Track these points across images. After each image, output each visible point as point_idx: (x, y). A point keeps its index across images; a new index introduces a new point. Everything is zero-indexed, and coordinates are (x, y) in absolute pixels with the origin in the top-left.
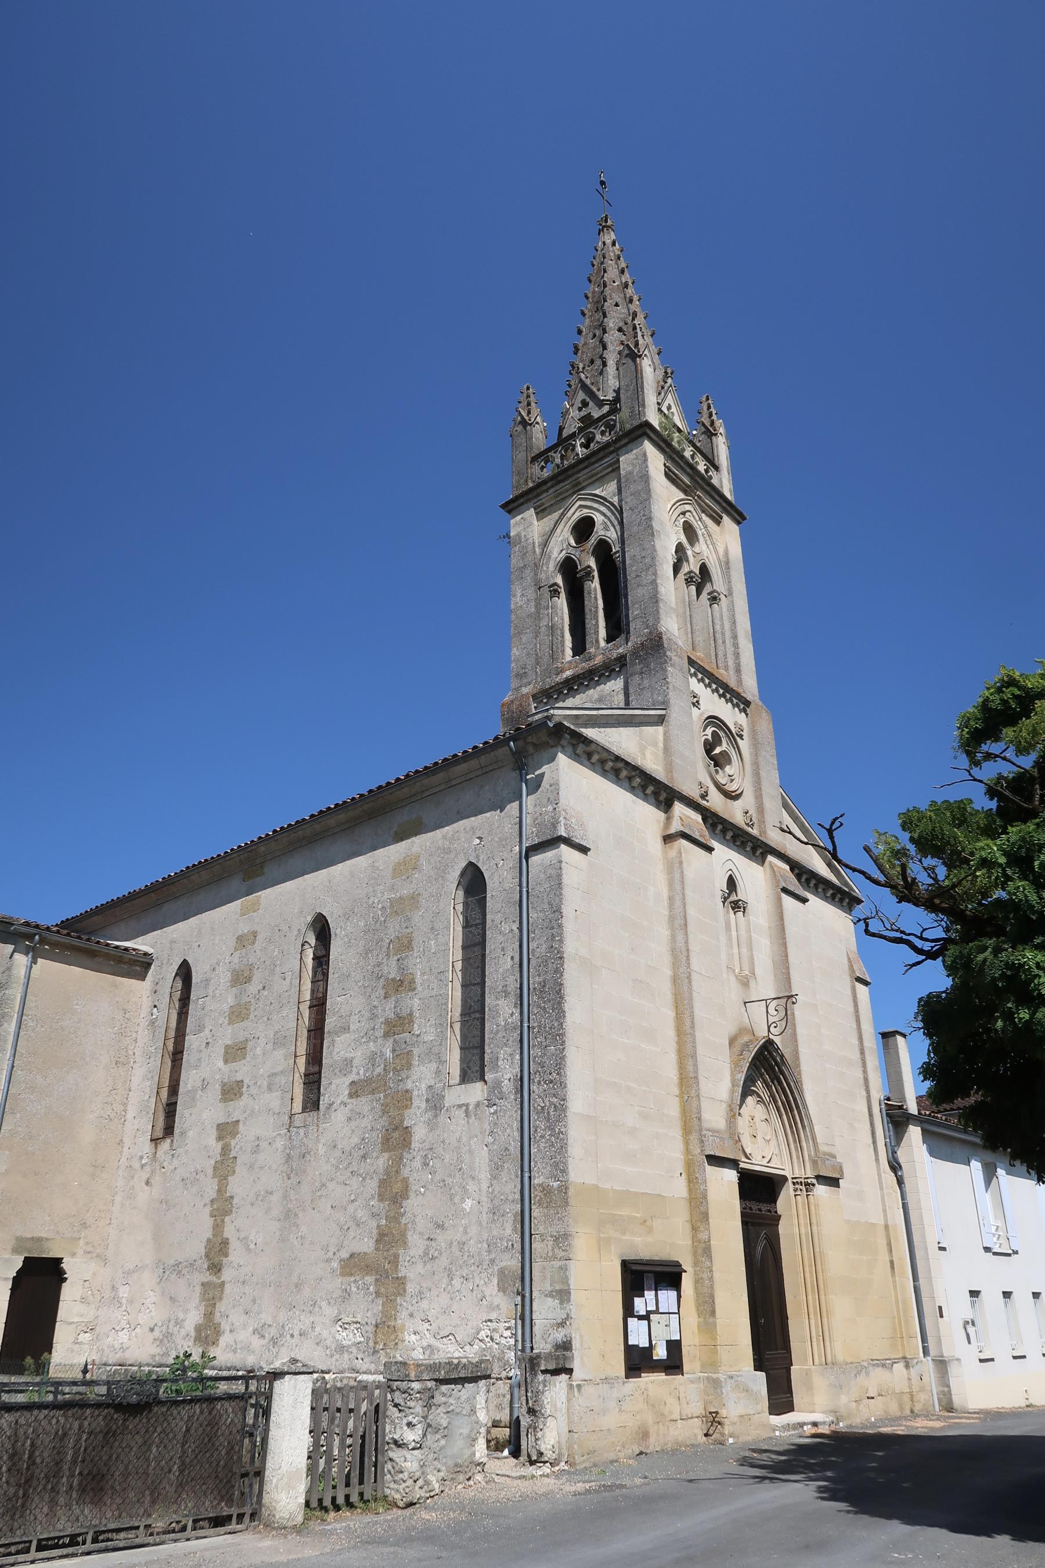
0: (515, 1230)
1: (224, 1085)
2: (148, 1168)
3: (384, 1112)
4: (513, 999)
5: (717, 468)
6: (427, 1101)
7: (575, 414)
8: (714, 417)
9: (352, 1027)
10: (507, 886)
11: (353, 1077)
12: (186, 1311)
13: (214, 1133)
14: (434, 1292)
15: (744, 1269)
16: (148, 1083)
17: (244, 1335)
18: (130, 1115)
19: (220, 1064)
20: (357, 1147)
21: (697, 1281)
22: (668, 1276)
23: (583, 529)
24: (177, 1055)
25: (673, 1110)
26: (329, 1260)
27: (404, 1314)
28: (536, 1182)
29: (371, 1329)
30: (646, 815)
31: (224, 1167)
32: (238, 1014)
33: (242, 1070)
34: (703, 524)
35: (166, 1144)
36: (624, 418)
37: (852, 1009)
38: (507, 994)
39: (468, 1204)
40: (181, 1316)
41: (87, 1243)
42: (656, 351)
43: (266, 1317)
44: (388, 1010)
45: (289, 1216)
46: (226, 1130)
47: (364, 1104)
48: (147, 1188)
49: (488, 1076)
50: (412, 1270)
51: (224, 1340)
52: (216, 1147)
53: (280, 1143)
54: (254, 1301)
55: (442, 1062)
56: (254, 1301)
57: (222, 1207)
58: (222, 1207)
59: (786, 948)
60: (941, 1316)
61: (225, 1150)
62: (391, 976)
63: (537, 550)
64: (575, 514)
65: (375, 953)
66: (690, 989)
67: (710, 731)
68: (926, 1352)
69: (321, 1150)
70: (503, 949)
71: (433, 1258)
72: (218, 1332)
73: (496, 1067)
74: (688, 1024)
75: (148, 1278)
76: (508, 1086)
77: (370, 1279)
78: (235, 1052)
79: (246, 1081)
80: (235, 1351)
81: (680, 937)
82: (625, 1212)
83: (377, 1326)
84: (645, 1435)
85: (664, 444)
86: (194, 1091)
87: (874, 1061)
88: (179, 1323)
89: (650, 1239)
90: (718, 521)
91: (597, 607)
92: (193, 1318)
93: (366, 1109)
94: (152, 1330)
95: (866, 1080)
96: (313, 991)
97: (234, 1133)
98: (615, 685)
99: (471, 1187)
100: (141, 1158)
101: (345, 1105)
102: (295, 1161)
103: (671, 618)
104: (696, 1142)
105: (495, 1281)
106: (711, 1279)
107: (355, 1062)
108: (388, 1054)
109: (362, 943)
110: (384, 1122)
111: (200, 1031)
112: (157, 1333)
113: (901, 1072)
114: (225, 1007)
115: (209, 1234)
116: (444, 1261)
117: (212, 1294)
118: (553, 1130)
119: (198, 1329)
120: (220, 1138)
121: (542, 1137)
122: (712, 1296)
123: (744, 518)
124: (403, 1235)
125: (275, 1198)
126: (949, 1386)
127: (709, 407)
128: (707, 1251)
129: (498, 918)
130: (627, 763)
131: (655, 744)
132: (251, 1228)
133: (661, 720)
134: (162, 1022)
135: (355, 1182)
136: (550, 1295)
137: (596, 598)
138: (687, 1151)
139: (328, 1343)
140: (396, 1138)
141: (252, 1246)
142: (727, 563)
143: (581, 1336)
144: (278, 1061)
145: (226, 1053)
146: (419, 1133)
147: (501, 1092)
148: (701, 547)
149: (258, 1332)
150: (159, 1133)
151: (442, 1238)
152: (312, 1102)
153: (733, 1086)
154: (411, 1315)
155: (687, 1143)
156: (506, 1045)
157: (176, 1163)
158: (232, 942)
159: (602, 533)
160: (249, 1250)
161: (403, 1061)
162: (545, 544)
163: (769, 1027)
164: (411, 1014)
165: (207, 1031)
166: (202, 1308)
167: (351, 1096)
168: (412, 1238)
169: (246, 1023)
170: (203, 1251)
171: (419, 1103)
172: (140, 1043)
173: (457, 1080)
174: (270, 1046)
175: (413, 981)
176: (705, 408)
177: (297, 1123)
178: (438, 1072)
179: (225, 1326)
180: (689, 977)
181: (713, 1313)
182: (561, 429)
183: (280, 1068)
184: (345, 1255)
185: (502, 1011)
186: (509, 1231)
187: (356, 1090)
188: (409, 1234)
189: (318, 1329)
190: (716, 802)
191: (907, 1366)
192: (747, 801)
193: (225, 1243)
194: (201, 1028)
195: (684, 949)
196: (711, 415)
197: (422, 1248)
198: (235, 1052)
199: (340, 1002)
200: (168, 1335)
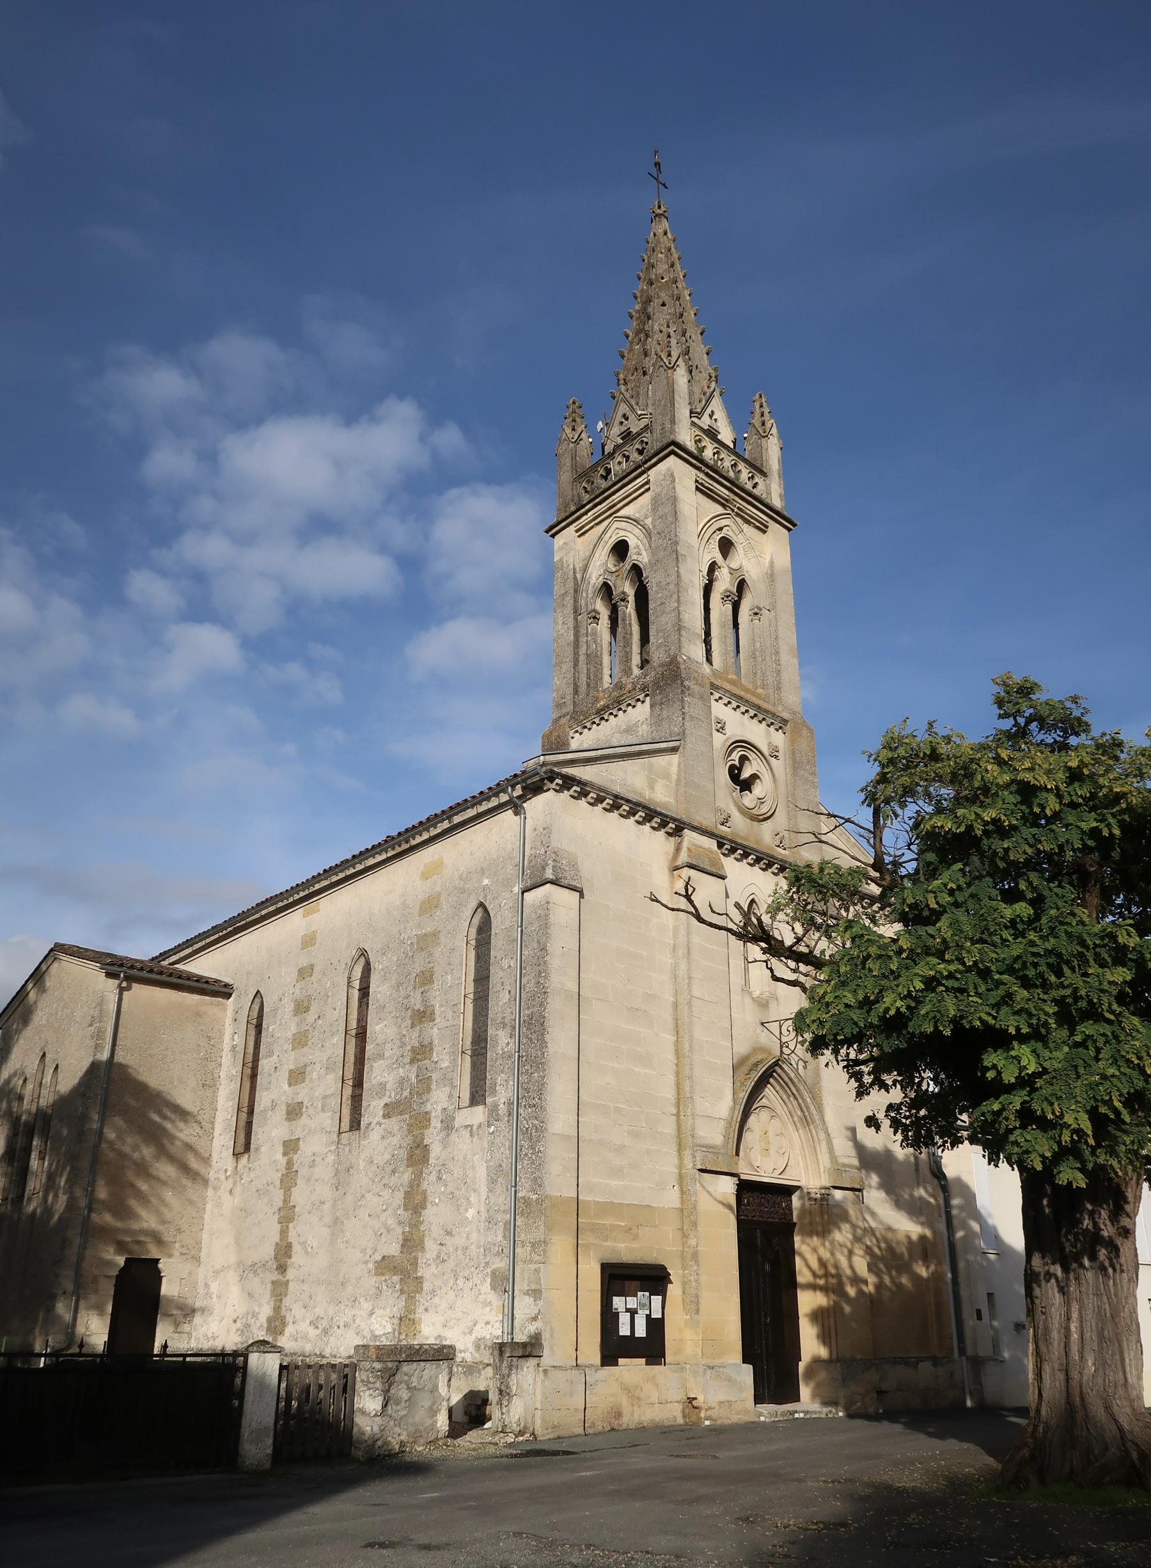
0: (504, 1237)
1: (288, 1105)
2: (230, 1180)
3: (410, 1131)
4: (508, 1029)
5: (764, 474)
6: (442, 1121)
7: (616, 430)
8: (767, 416)
9: (387, 1054)
10: (507, 924)
11: (386, 1100)
12: (260, 1306)
13: (281, 1149)
14: (444, 1290)
16: (231, 1104)
17: (304, 1326)
18: (216, 1133)
19: (286, 1087)
20: (388, 1163)
21: (685, 1284)
22: (654, 1279)
23: (621, 549)
24: (254, 1076)
25: (668, 1127)
26: (366, 1262)
27: (421, 1309)
28: (520, 1195)
29: (396, 1321)
30: (654, 845)
31: (289, 1178)
32: (300, 1041)
33: (302, 1093)
34: (743, 536)
35: (244, 1160)
36: (654, 441)
38: (504, 1025)
39: (470, 1213)
40: (257, 1309)
41: (183, 1246)
42: (705, 351)
43: (319, 1311)
44: (413, 1039)
45: (336, 1223)
46: (291, 1147)
47: (394, 1124)
48: (231, 1198)
49: (489, 1100)
50: (428, 1272)
51: (289, 1330)
52: (283, 1161)
53: (331, 1158)
54: (311, 1297)
55: (453, 1087)
56: (311, 1297)
57: (287, 1214)
58: (287, 1214)
61: (290, 1164)
62: (417, 1008)
63: (579, 576)
64: (611, 539)
65: (405, 986)
67: (736, 756)
68: (962, 1351)
69: (362, 1164)
70: (502, 984)
71: (443, 1261)
72: (284, 1324)
73: (494, 1092)
74: (687, 1047)
75: (232, 1276)
76: (502, 1109)
77: (396, 1278)
78: (297, 1076)
79: (305, 1103)
80: (296, 1340)
81: (683, 966)
82: (608, 1221)
83: (401, 1319)
84: (619, 1415)
85: (695, 460)
86: (265, 1111)
88: (255, 1315)
89: (634, 1245)
90: (763, 529)
91: (631, 634)
92: (266, 1311)
93: (396, 1128)
94: (235, 1321)
96: (358, 1020)
97: (296, 1149)
98: (641, 712)
99: (473, 1198)
100: (226, 1171)
101: (380, 1124)
102: (343, 1173)
103: (695, 644)
104: (690, 1157)
105: (489, 1280)
106: (697, 1281)
107: (389, 1086)
108: (414, 1079)
109: (395, 976)
110: (409, 1140)
111: (269, 1056)
112: (239, 1324)
114: (289, 1035)
115: (277, 1239)
116: (451, 1263)
117: (279, 1290)
118: (534, 1149)
119: (270, 1321)
120: (285, 1154)
121: (526, 1155)
122: (697, 1296)
123: (794, 525)
124: (422, 1241)
125: (327, 1206)
127: (761, 406)
128: (695, 1256)
129: (500, 955)
130: (628, 801)
131: (667, 776)
132: (309, 1233)
133: (674, 750)
134: (240, 1049)
135: (386, 1193)
136: (527, 1293)
137: (630, 624)
138: (681, 1166)
139: (365, 1333)
140: (418, 1155)
141: (309, 1249)
142: (772, 575)
143: (552, 1329)
144: (326, 1085)
145: (290, 1076)
146: (436, 1151)
147: (498, 1115)
148: (740, 558)
149: (314, 1324)
150: (240, 1149)
151: (449, 1241)
152: (355, 1124)
154: (426, 1310)
155: (680, 1157)
156: (502, 1072)
157: (252, 1175)
158: (295, 975)
159: (635, 557)
160: (307, 1253)
161: (424, 1085)
162: (585, 569)
163: (781, 1047)
164: (431, 1043)
165: (275, 1057)
166: (272, 1303)
167: (384, 1116)
168: (429, 1243)
169: (305, 1049)
170: (273, 1254)
171: (436, 1123)
172: (224, 1068)
173: (467, 1104)
174: (323, 1071)
175: (433, 1013)
176: (757, 407)
177: (344, 1141)
178: (450, 1096)
179: (289, 1319)
180: (690, 1004)
181: (698, 1311)
182: (603, 446)
183: (330, 1092)
184: (379, 1258)
185: (501, 1041)
186: (500, 1238)
187: (389, 1111)
188: (426, 1239)
189: (357, 1321)
190: (739, 826)
192: (780, 821)
193: (289, 1246)
194: (270, 1054)
195: (686, 976)
196: (762, 415)
197: (435, 1253)
198: (297, 1076)
199: (377, 1029)
200: (247, 1326)
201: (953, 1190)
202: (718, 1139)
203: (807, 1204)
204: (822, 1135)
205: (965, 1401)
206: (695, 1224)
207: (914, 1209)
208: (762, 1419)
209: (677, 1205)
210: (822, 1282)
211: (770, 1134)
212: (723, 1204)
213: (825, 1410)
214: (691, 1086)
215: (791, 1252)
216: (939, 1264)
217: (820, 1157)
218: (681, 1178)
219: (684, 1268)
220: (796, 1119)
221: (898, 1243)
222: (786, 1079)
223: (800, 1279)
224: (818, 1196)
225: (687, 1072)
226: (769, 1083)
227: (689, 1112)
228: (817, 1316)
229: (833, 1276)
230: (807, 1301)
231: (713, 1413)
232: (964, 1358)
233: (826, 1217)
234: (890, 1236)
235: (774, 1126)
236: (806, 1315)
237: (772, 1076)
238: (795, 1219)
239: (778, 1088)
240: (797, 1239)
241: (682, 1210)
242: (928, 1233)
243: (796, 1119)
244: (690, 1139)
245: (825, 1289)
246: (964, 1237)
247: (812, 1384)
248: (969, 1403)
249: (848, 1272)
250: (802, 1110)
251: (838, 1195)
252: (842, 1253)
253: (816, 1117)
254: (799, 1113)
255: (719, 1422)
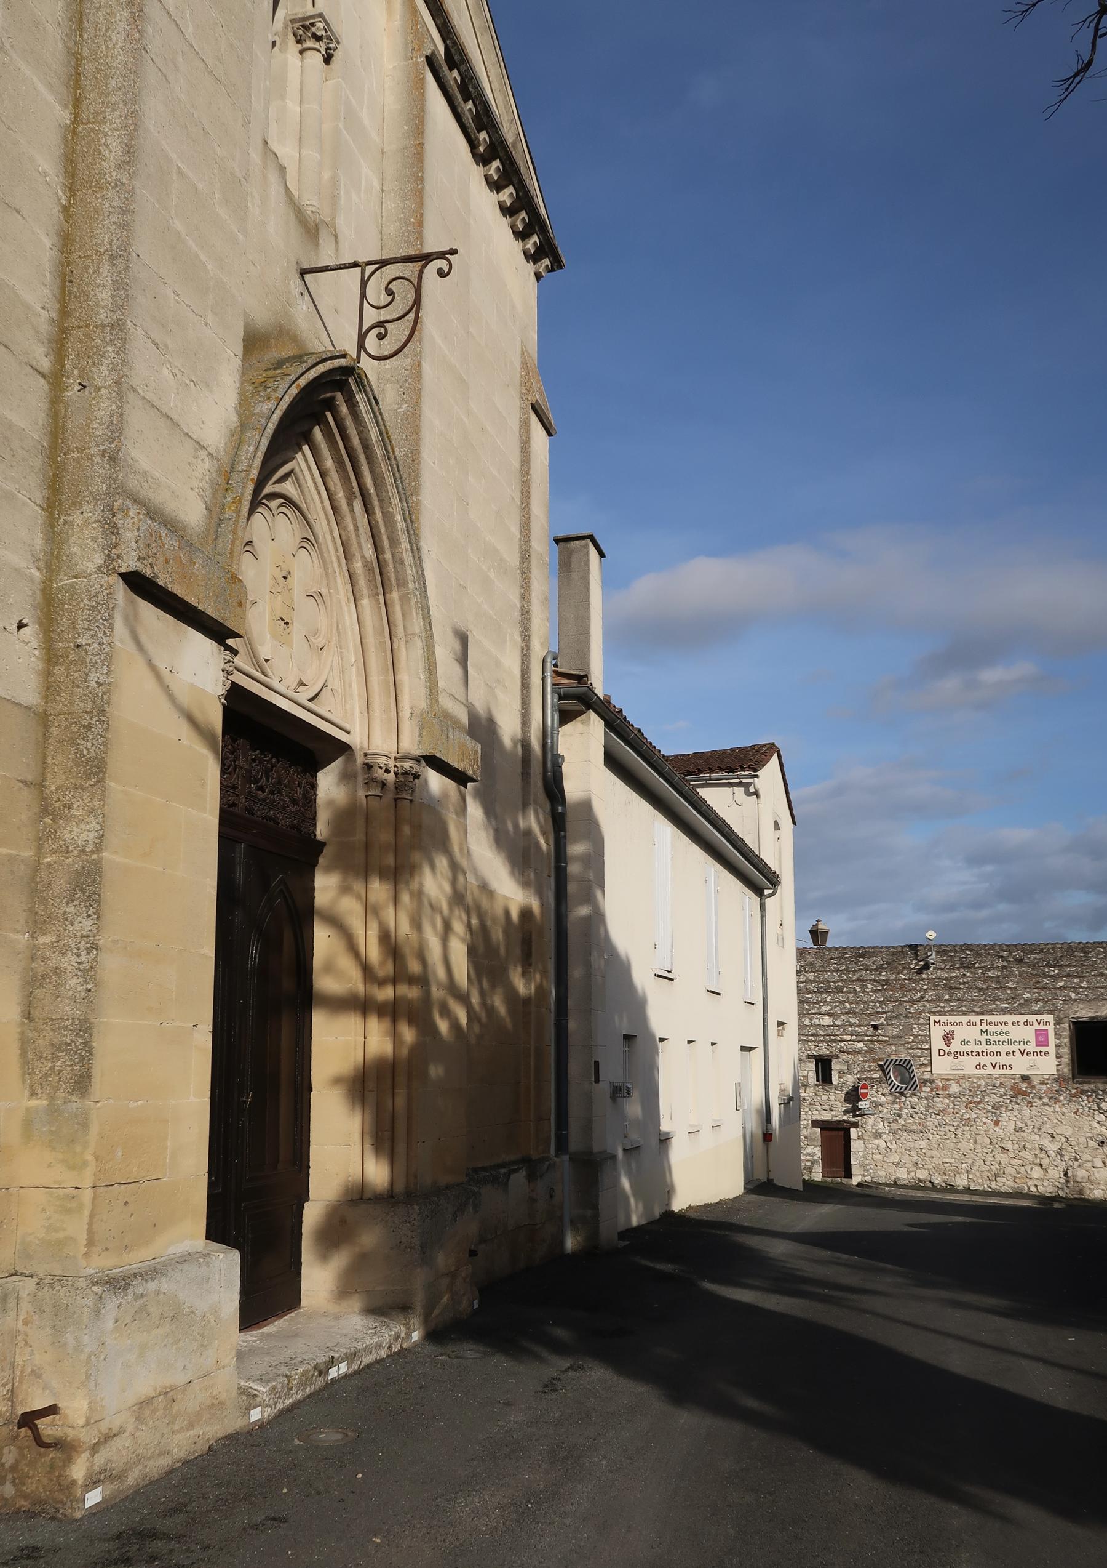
15: (209, 950)
37: (516, 463)
59: (421, 204)
60: (597, 1081)
66: (138, 47)
87: (542, 584)
95: (525, 614)
104: (93, 531)
106: (89, 973)
113: (588, 618)
122: (85, 1028)
126: (595, 1207)
128: (88, 885)
138: (53, 560)
153: (243, 426)
181: (82, 1083)
191: (531, 1177)
201: (571, 826)
202: (192, 512)
203: (361, 793)
204: (417, 625)
205: (562, 1242)
206: (95, 770)
207: (520, 855)
208: (256, 1415)
209: (29, 693)
210: (386, 994)
211: (295, 581)
212: (191, 720)
213: (387, 1335)
214: (120, 286)
215: (302, 914)
216: (544, 973)
217: (404, 677)
218: (50, 607)
219: (37, 925)
220: (358, 565)
221: (494, 919)
222: (356, 442)
223: (324, 983)
224: (391, 777)
225: (105, 236)
226: (308, 439)
227: (102, 374)
228: (368, 1085)
229: (412, 980)
230: (338, 1045)
231: (113, 1454)
232: (566, 1158)
233: (407, 830)
234: (485, 903)
235: (305, 568)
236: (337, 1081)
237: (321, 421)
238: (322, 831)
239: (329, 463)
240: (326, 886)
241: (46, 715)
242: (535, 905)
243: (358, 565)
244: (100, 467)
245: (392, 1012)
246: (588, 920)
247: (340, 1260)
248: (570, 1243)
249: (441, 973)
250: (377, 548)
251: (435, 781)
252: (434, 926)
253: (410, 572)
254: (369, 551)
255: (133, 1477)
